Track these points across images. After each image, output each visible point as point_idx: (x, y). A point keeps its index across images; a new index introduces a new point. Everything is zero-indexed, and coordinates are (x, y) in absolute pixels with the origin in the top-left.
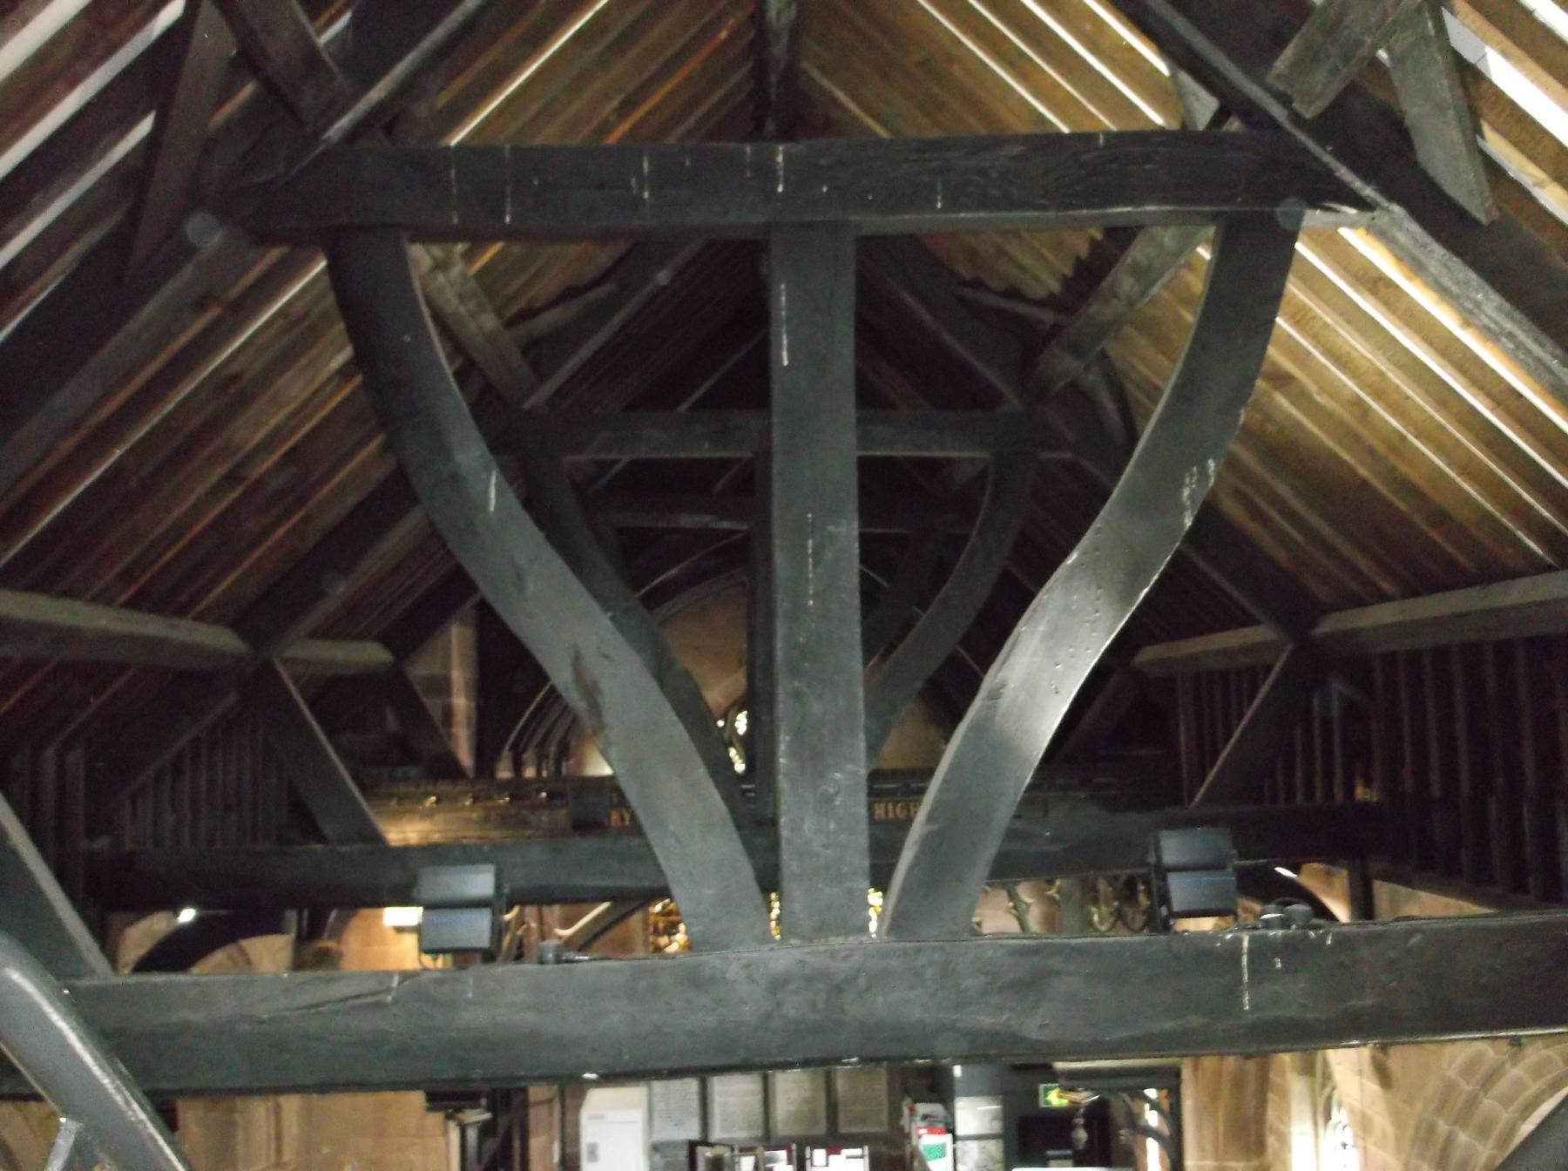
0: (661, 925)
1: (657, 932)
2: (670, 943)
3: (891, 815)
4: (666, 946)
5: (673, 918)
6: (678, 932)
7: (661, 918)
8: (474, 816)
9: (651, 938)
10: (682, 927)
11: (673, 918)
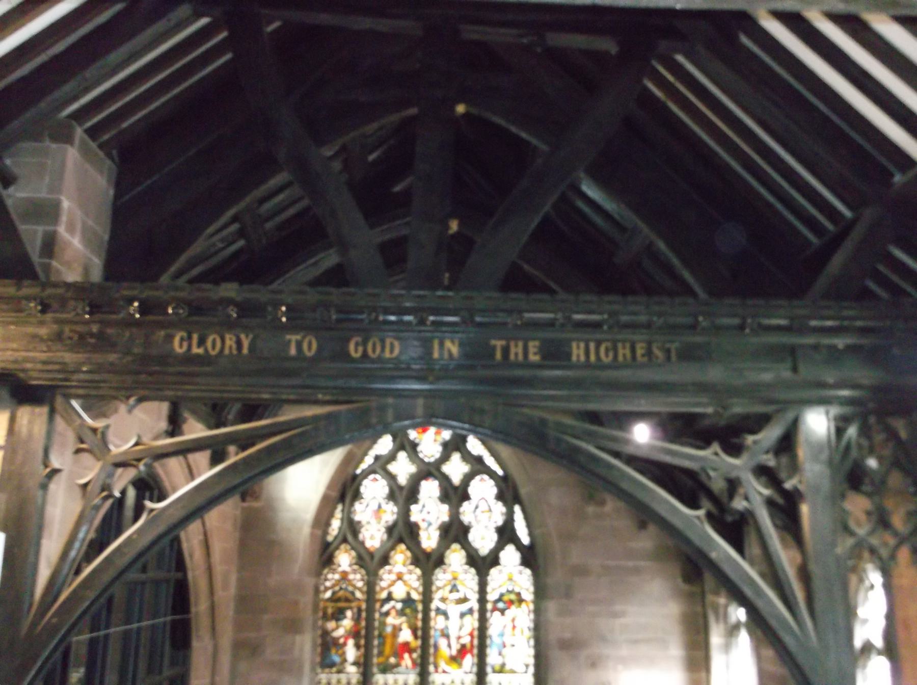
0: (330, 611)
1: (326, 617)
2: (337, 627)
3: (593, 358)
4: (333, 630)
5: (342, 604)
6: (345, 617)
7: (330, 605)
8: (43, 331)
9: (320, 623)
10: (349, 614)
11: (342, 604)
